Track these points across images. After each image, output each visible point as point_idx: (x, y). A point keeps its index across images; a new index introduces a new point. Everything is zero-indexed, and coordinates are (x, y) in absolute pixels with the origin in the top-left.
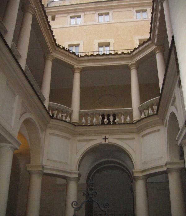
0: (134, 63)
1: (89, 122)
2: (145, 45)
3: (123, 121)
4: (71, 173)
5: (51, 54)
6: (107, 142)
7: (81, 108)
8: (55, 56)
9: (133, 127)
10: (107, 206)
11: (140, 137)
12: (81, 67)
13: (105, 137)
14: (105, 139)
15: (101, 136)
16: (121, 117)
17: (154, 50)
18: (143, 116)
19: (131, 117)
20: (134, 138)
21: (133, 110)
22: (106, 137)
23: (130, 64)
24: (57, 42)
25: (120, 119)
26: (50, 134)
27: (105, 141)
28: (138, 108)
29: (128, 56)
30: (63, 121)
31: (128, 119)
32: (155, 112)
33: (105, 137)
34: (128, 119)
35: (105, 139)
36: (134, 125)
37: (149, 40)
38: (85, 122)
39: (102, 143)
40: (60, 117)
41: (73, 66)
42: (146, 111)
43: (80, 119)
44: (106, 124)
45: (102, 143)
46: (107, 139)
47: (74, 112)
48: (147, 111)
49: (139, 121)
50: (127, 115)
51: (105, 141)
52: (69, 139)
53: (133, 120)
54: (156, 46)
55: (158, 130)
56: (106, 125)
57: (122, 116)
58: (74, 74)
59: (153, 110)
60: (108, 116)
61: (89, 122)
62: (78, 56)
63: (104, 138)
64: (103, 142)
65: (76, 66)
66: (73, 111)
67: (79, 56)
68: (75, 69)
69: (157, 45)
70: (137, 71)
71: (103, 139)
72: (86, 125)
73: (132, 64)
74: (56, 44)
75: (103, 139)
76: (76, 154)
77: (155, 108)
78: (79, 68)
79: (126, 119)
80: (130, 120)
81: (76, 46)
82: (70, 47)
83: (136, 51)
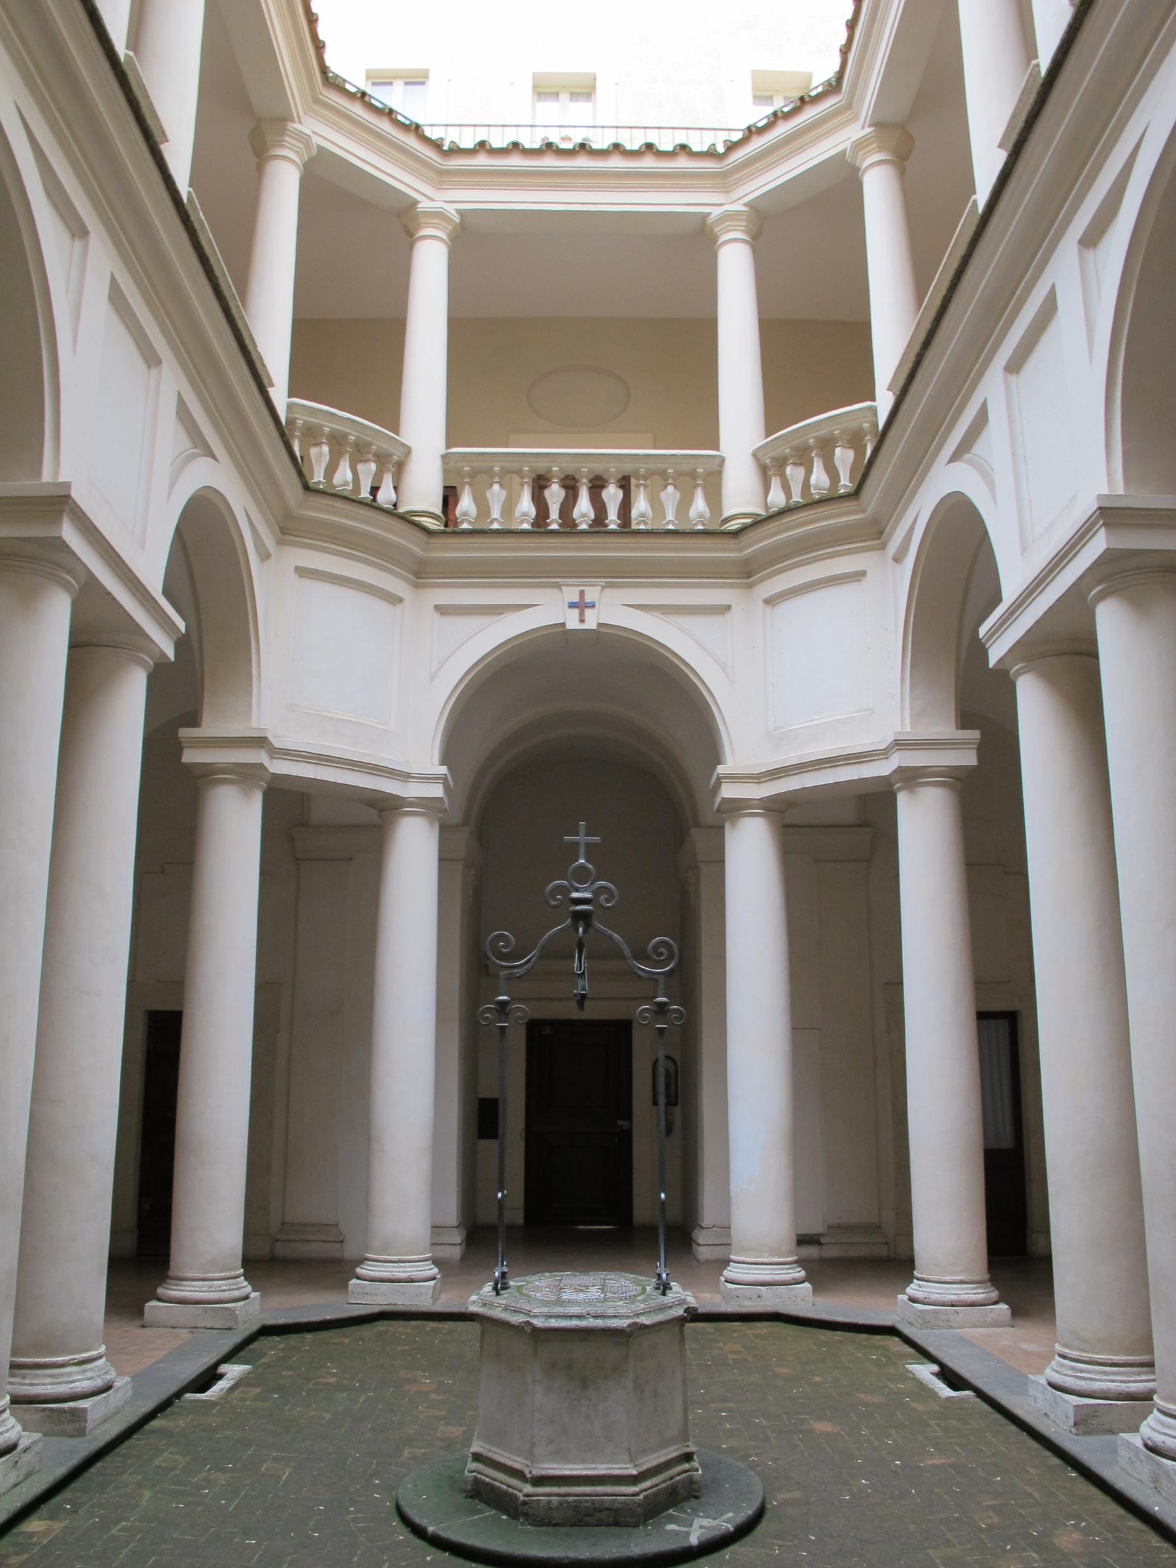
0: (739, 207)
1: (496, 513)
2: (810, 113)
3: (670, 520)
4: (405, 777)
5: (297, 126)
6: (591, 624)
7: (455, 432)
8: (316, 140)
9: (726, 552)
10: (661, 954)
11: (760, 604)
12: (451, 209)
13: (582, 594)
14: (581, 606)
15: (558, 586)
16: (662, 495)
17: (859, 145)
18: (777, 498)
19: (714, 497)
20: (728, 608)
21: (723, 460)
22: (588, 599)
23: (716, 212)
24: (330, 59)
25: (656, 504)
26: (302, 572)
27: (582, 621)
28: (754, 455)
29: (709, 165)
30: (361, 503)
31: (699, 505)
32: (846, 483)
33: (582, 594)
34: (699, 505)
35: (581, 606)
36: (731, 543)
37: (834, 86)
38: (473, 511)
39: (563, 624)
40: (346, 483)
41: (415, 203)
42: (794, 473)
43: (450, 497)
44: (584, 527)
45: (563, 624)
46: (592, 606)
47: (415, 456)
48: (800, 472)
49: (758, 522)
50: (696, 486)
51: (582, 621)
52: (396, 600)
53: (727, 513)
54: (868, 130)
55: (858, 576)
56: (582, 532)
57: (670, 489)
58: (411, 247)
59: (832, 471)
60: (597, 486)
61: (496, 513)
62: (436, 145)
63: (576, 599)
64: (573, 623)
65: (424, 205)
66: (408, 451)
67: (446, 148)
68: (422, 220)
69: (879, 125)
70: (754, 251)
71: (572, 605)
72: (478, 527)
73: (726, 217)
74: (324, 70)
75: (572, 605)
76: (432, 679)
77: (844, 457)
78: (440, 215)
79: (685, 503)
80: (708, 514)
81: (406, 84)
82: (374, 84)
83: (757, 144)
